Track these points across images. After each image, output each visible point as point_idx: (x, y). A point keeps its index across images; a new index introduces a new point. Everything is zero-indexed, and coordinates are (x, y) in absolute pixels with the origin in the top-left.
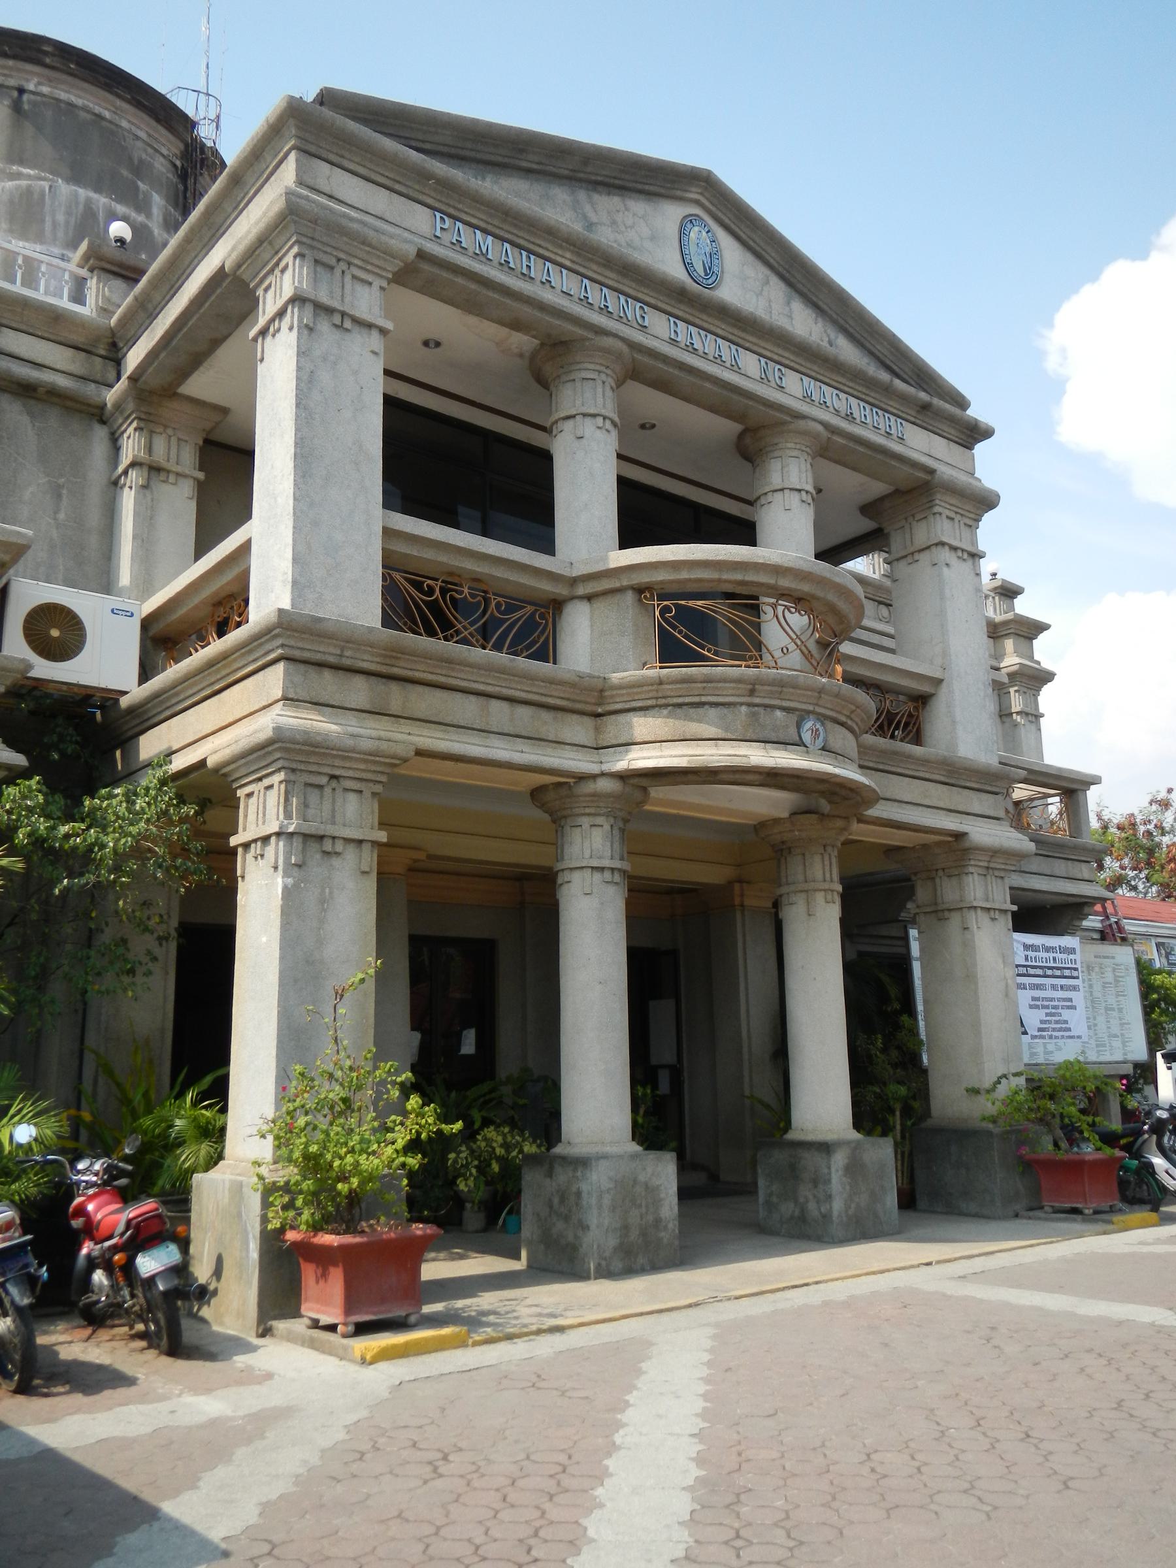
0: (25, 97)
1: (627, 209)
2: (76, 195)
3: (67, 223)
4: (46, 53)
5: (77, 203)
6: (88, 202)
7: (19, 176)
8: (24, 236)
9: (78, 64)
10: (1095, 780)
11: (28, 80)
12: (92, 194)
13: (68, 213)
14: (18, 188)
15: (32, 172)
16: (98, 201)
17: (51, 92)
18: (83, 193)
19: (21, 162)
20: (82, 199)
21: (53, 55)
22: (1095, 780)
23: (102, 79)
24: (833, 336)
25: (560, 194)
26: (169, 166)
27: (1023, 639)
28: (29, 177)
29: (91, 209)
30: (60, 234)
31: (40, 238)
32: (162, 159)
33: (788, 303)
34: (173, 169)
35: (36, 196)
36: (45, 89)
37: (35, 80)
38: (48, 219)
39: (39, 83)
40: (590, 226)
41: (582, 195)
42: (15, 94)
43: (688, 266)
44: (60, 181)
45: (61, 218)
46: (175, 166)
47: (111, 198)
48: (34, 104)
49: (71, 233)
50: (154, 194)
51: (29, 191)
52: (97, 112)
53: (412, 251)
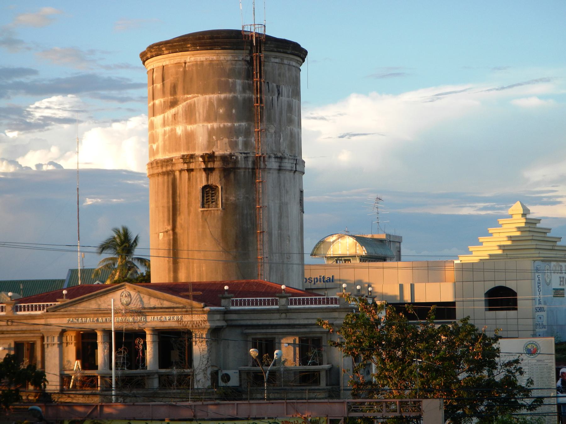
1: (108, 298)
2: (205, 99)
3: (203, 111)
4: (189, 47)
5: (206, 102)
6: (210, 99)
7: (187, 99)
8: (190, 123)
9: (199, 46)
12: (212, 96)
13: (204, 108)
14: (187, 103)
16: (213, 97)
17: (194, 59)
18: (207, 97)
19: (188, 93)
20: (208, 100)
21: (191, 47)
23: (209, 47)
24: (162, 302)
25: (93, 302)
26: (243, 63)
27: (344, 312)
28: (190, 98)
29: (211, 102)
30: (201, 117)
31: (195, 122)
32: (240, 62)
33: (149, 300)
34: (246, 63)
35: (193, 105)
37: (189, 57)
39: (190, 57)
40: (99, 305)
41: (98, 300)
42: (184, 64)
43: (122, 304)
44: (200, 95)
45: (201, 111)
46: (246, 61)
47: (219, 94)
48: (189, 66)
49: (205, 115)
50: (237, 80)
52: (211, 59)
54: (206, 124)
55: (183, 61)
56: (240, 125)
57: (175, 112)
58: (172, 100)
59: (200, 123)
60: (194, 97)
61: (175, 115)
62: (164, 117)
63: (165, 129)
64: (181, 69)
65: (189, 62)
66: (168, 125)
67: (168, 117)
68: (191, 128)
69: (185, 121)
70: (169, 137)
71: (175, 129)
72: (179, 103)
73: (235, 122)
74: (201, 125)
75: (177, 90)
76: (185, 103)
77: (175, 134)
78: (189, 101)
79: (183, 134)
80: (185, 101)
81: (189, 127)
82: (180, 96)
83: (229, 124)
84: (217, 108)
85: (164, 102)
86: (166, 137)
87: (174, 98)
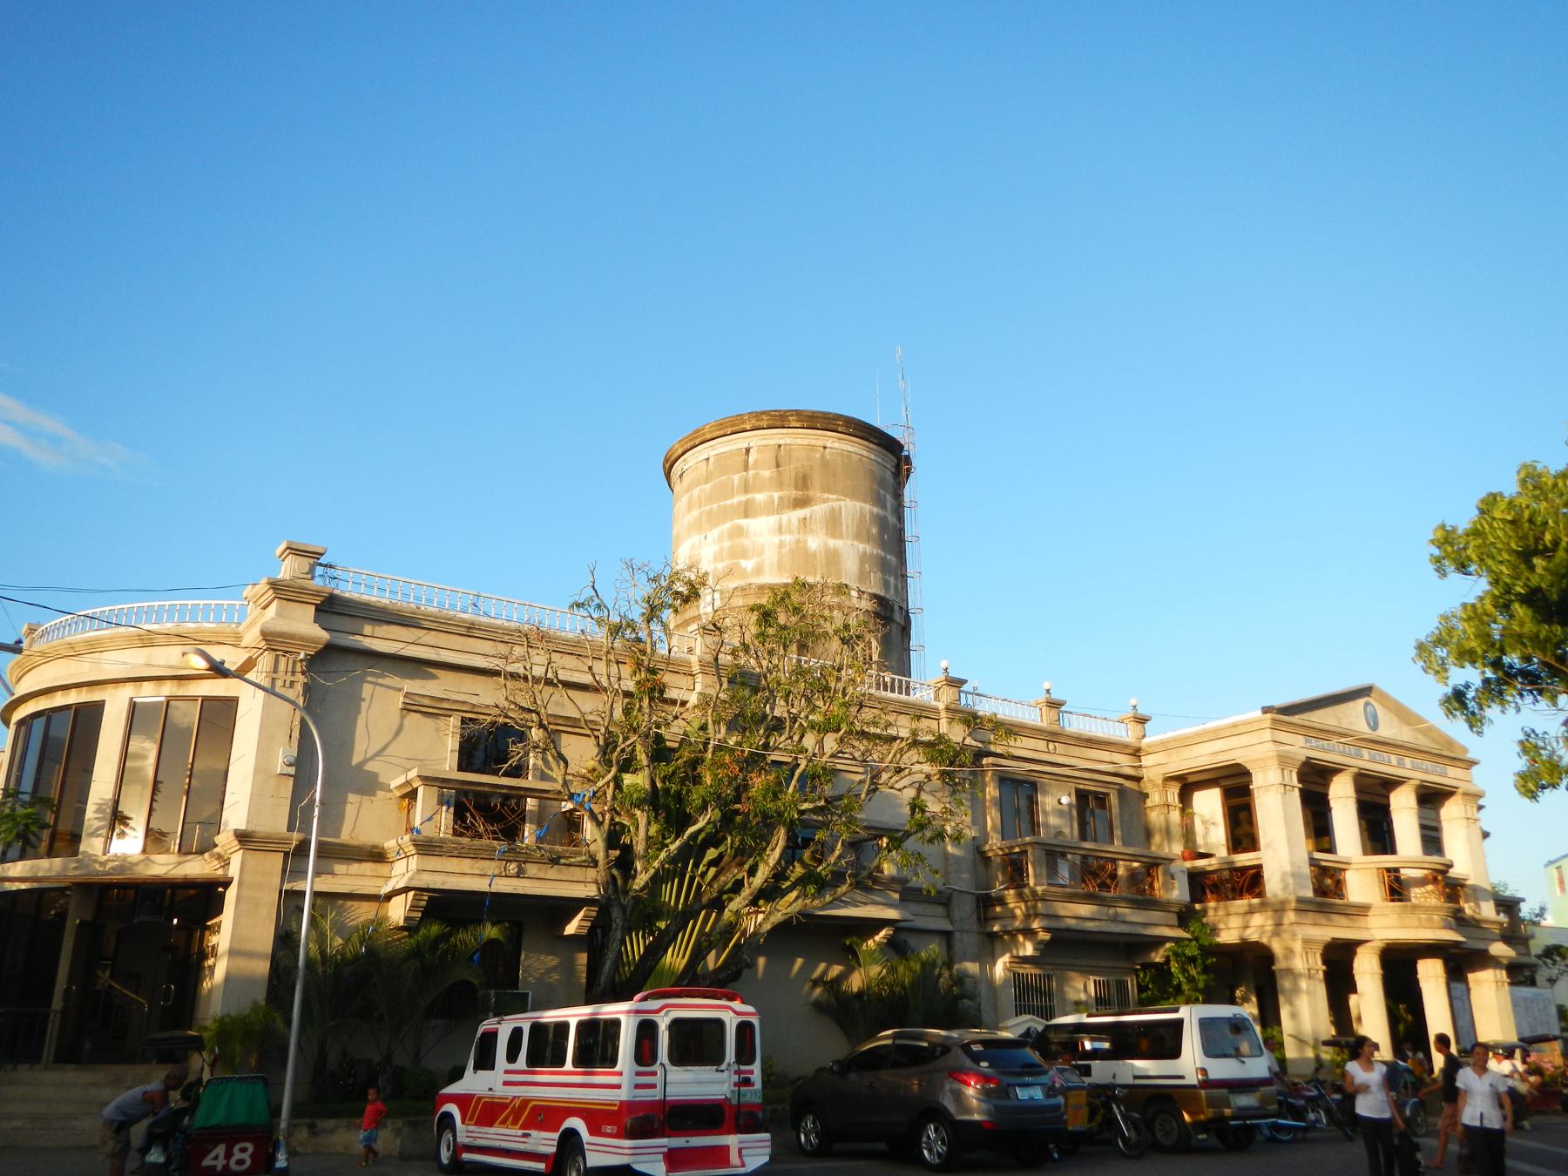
0: (827, 450)
3: (853, 524)
4: (839, 425)
8: (834, 537)
10: (1523, 900)
11: (827, 441)
15: (834, 497)
19: (829, 492)
22: (1523, 900)
36: (836, 445)
37: (830, 442)
38: (844, 524)
39: (833, 442)
42: (822, 449)
48: (832, 454)
51: (833, 510)
53: (1303, 759)
54: (856, 543)
55: (820, 443)
56: (891, 560)
57: (806, 515)
58: (799, 497)
59: (848, 539)
60: (838, 500)
61: (805, 519)
62: (780, 520)
63: (783, 538)
64: (818, 456)
65: (831, 448)
66: (790, 532)
67: (789, 521)
68: (834, 544)
69: (824, 531)
70: (792, 551)
71: (806, 542)
72: (813, 503)
73: (890, 554)
74: (849, 542)
75: (809, 483)
76: (824, 506)
77: (806, 548)
78: (830, 504)
79: (820, 551)
80: (824, 502)
81: (832, 543)
82: (815, 493)
83: (883, 554)
84: (870, 525)
85: (781, 498)
86: (784, 550)
87: (803, 495)
